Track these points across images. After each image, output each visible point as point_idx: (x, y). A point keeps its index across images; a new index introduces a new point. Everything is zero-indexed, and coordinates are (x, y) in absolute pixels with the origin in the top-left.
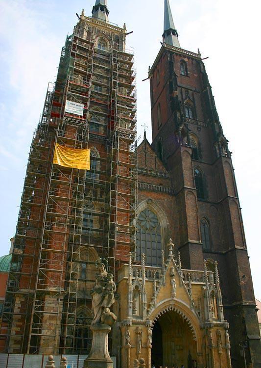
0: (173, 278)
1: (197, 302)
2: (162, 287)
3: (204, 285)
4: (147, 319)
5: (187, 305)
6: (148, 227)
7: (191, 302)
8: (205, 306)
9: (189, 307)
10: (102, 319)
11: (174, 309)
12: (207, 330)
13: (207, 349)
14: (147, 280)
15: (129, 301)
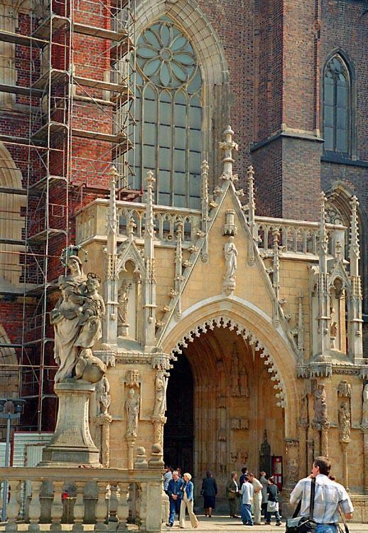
0: (229, 242)
1: (292, 307)
2: (200, 264)
3: (317, 262)
4: (156, 350)
5: (264, 315)
6: (166, 83)
7: (276, 306)
8: (315, 316)
9: (269, 319)
10: (77, 371)
11: (229, 325)
12: (314, 382)
13: (310, 429)
14: (158, 243)
15: (109, 302)
